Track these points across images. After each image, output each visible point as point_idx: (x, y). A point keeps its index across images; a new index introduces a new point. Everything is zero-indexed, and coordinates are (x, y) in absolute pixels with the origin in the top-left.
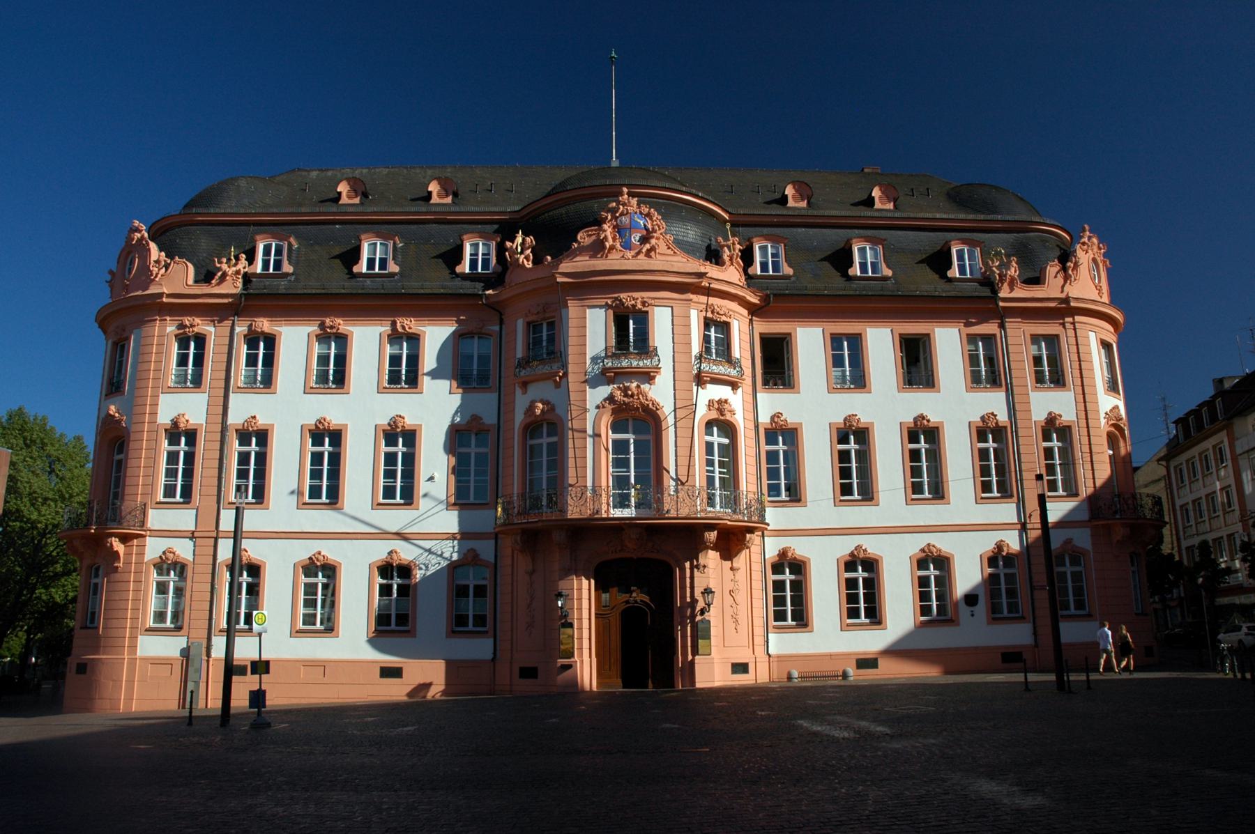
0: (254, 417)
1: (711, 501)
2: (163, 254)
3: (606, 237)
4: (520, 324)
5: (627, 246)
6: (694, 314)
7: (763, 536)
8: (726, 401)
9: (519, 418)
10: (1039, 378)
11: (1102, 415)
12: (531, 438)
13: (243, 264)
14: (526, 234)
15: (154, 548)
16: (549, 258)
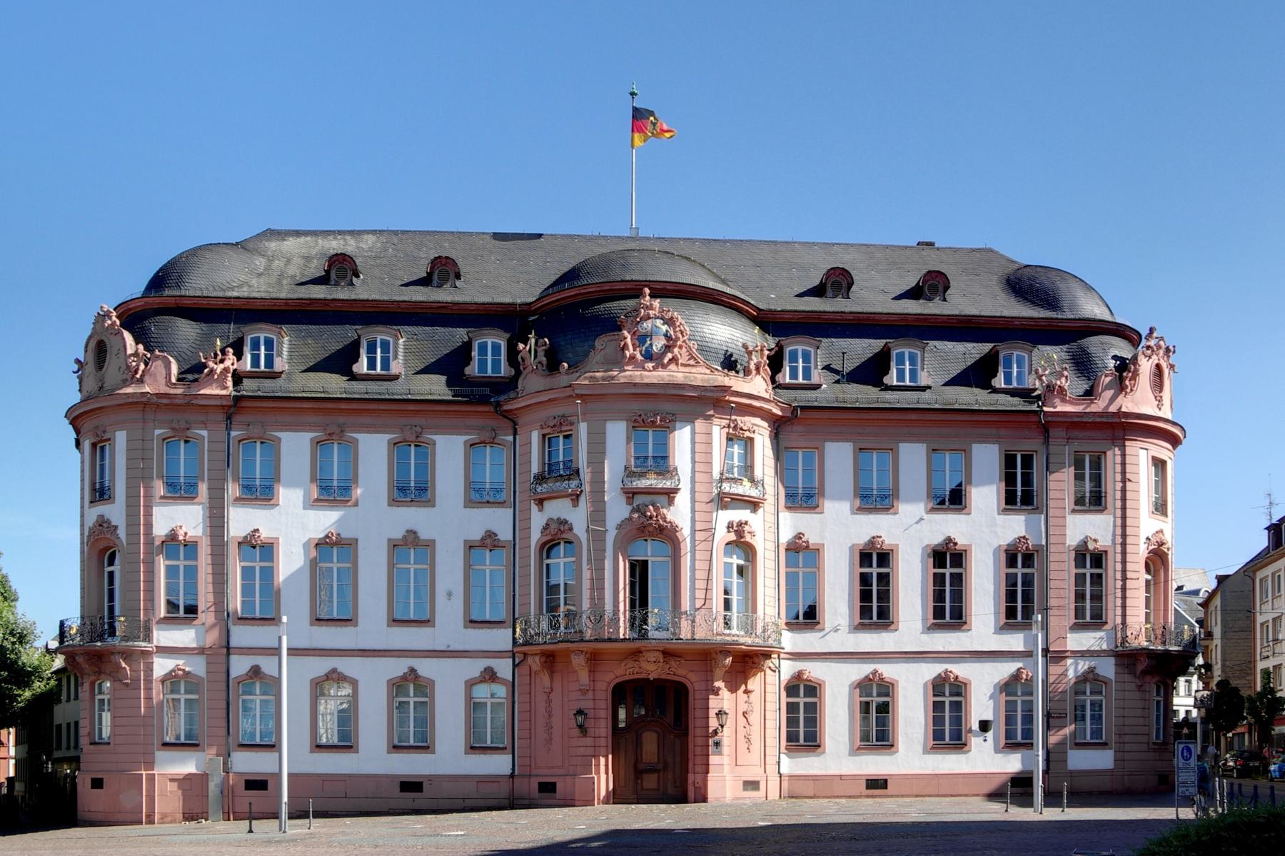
0: (257, 530)
1: (727, 624)
2: (141, 347)
3: (625, 344)
4: (535, 436)
5: (649, 356)
6: (716, 430)
8: (746, 523)
9: (536, 536)
12: (548, 557)
13: (230, 360)
14: (539, 336)
16: (566, 365)
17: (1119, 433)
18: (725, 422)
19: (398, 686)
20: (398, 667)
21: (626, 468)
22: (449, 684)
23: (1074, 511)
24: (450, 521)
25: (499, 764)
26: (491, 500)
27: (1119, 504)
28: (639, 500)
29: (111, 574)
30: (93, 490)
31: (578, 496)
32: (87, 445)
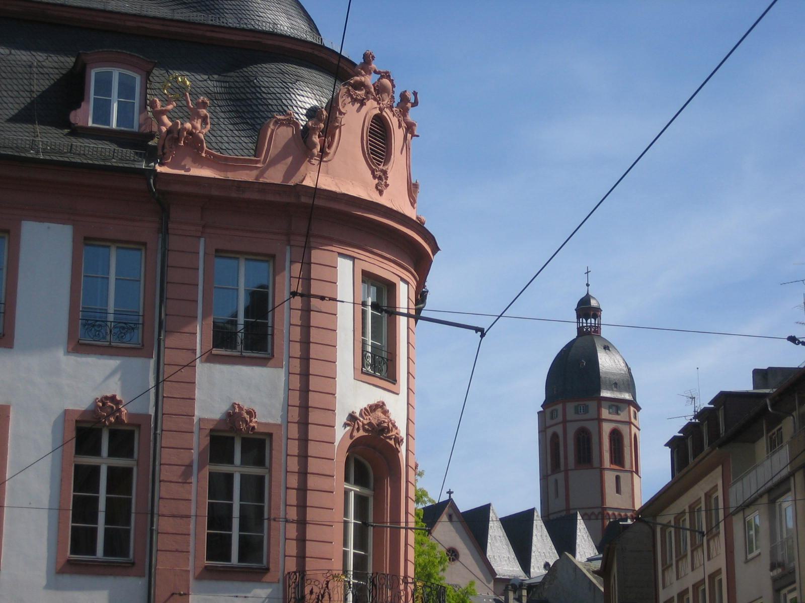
11: (341, 418)
23: (210, 358)
27: (296, 350)
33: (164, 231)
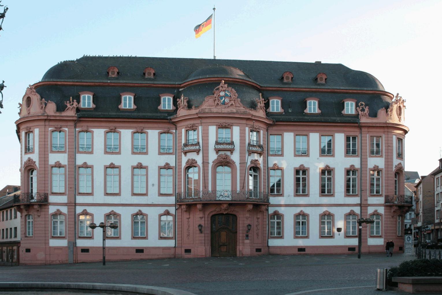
4: (183, 131)
7: (268, 207)
9: (184, 165)
10: (372, 152)
11: (394, 166)
13: (75, 103)
15: (52, 209)
17: (386, 130)
18: (250, 126)
19: (135, 216)
20: (135, 210)
21: (216, 142)
22: (153, 214)
23: (370, 157)
24: (153, 160)
25: (171, 243)
26: (167, 152)
28: (220, 153)
29: (32, 178)
30: (26, 149)
31: (199, 151)
32: (23, 134)
33: (361, 133)
